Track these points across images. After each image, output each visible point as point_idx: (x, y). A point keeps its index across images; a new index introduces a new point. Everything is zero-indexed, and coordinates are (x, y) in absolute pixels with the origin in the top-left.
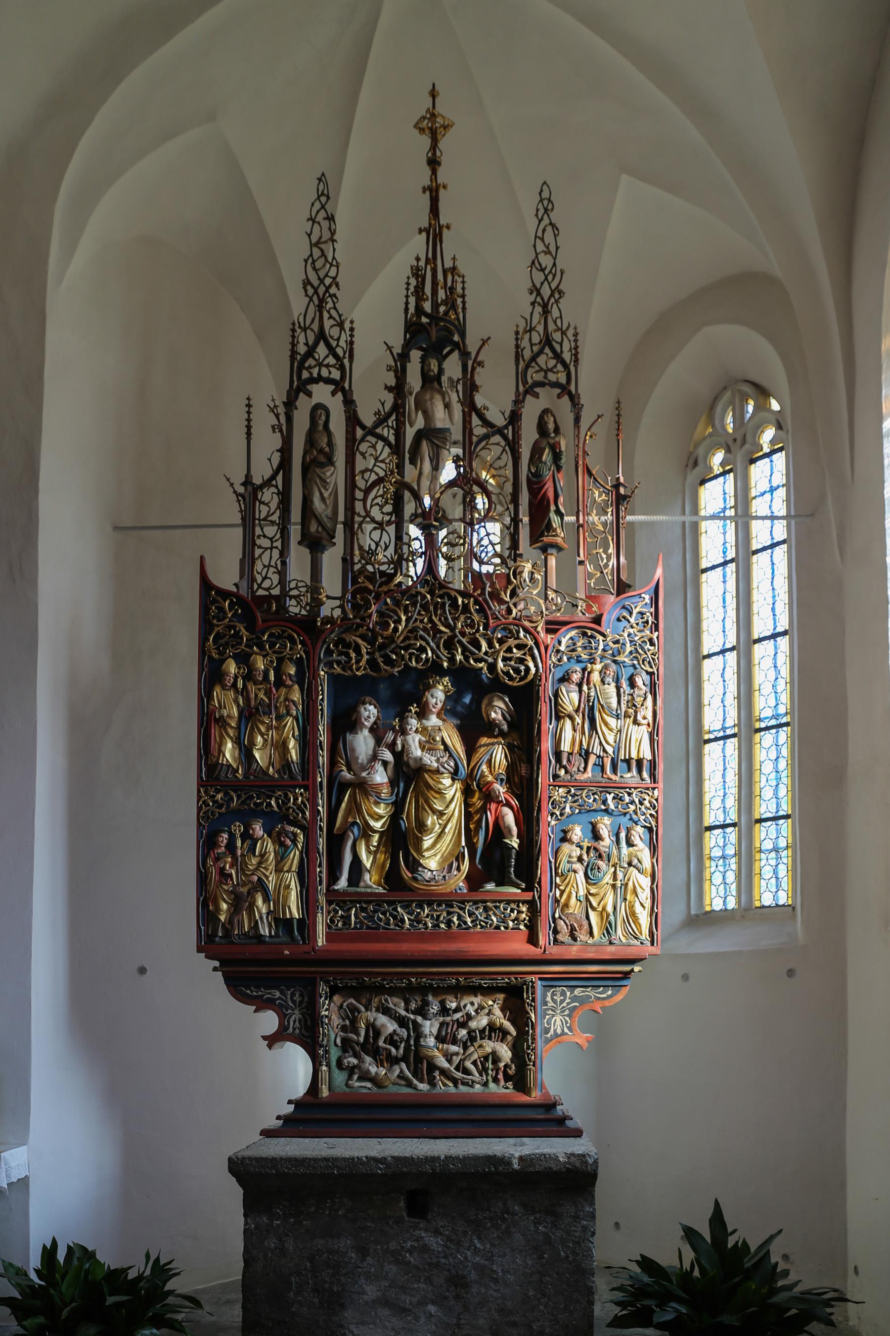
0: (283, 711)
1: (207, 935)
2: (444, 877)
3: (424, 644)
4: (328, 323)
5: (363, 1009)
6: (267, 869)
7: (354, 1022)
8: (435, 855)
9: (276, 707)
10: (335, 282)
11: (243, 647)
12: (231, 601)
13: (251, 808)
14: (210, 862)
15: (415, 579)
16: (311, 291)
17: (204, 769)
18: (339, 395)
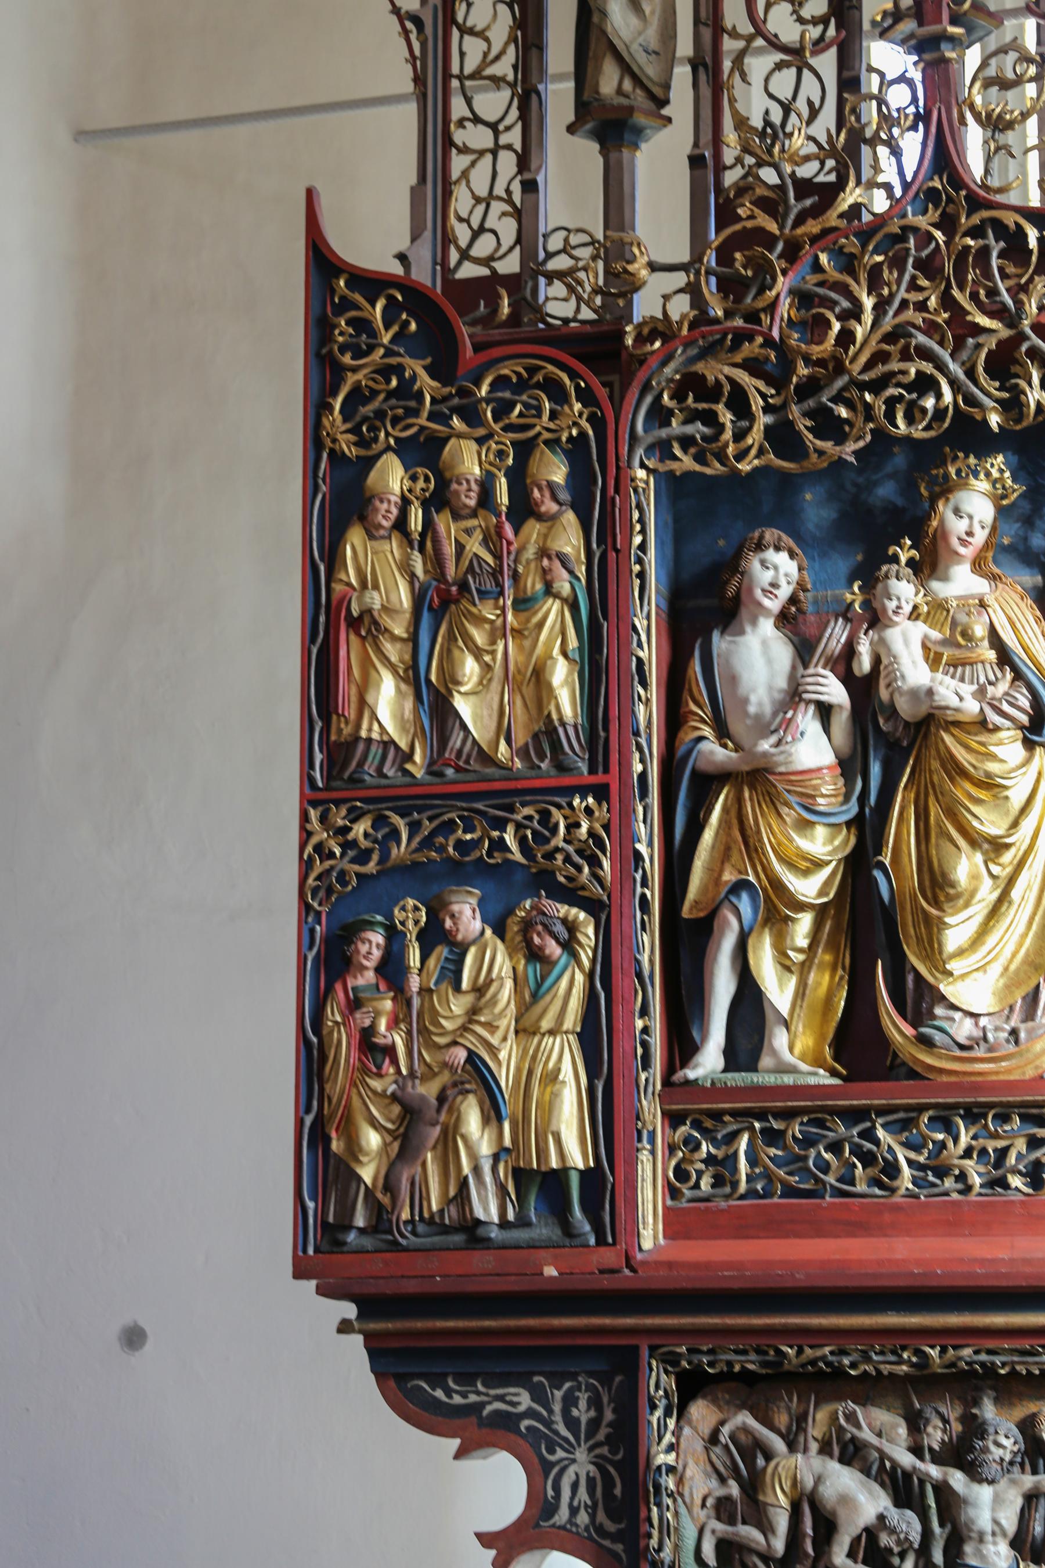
0: (533, 584)
1: (325, 1226)
2: (1014, 1032)
3: (928, 368)
5: (779, 1444)
6: (491, 1027)
7: (753, 1485)
9: (515, 576)
11: (423, 421)
12: (391, 299)
13: (450, 859)
14: (333, 1014)
15: (898, 192)
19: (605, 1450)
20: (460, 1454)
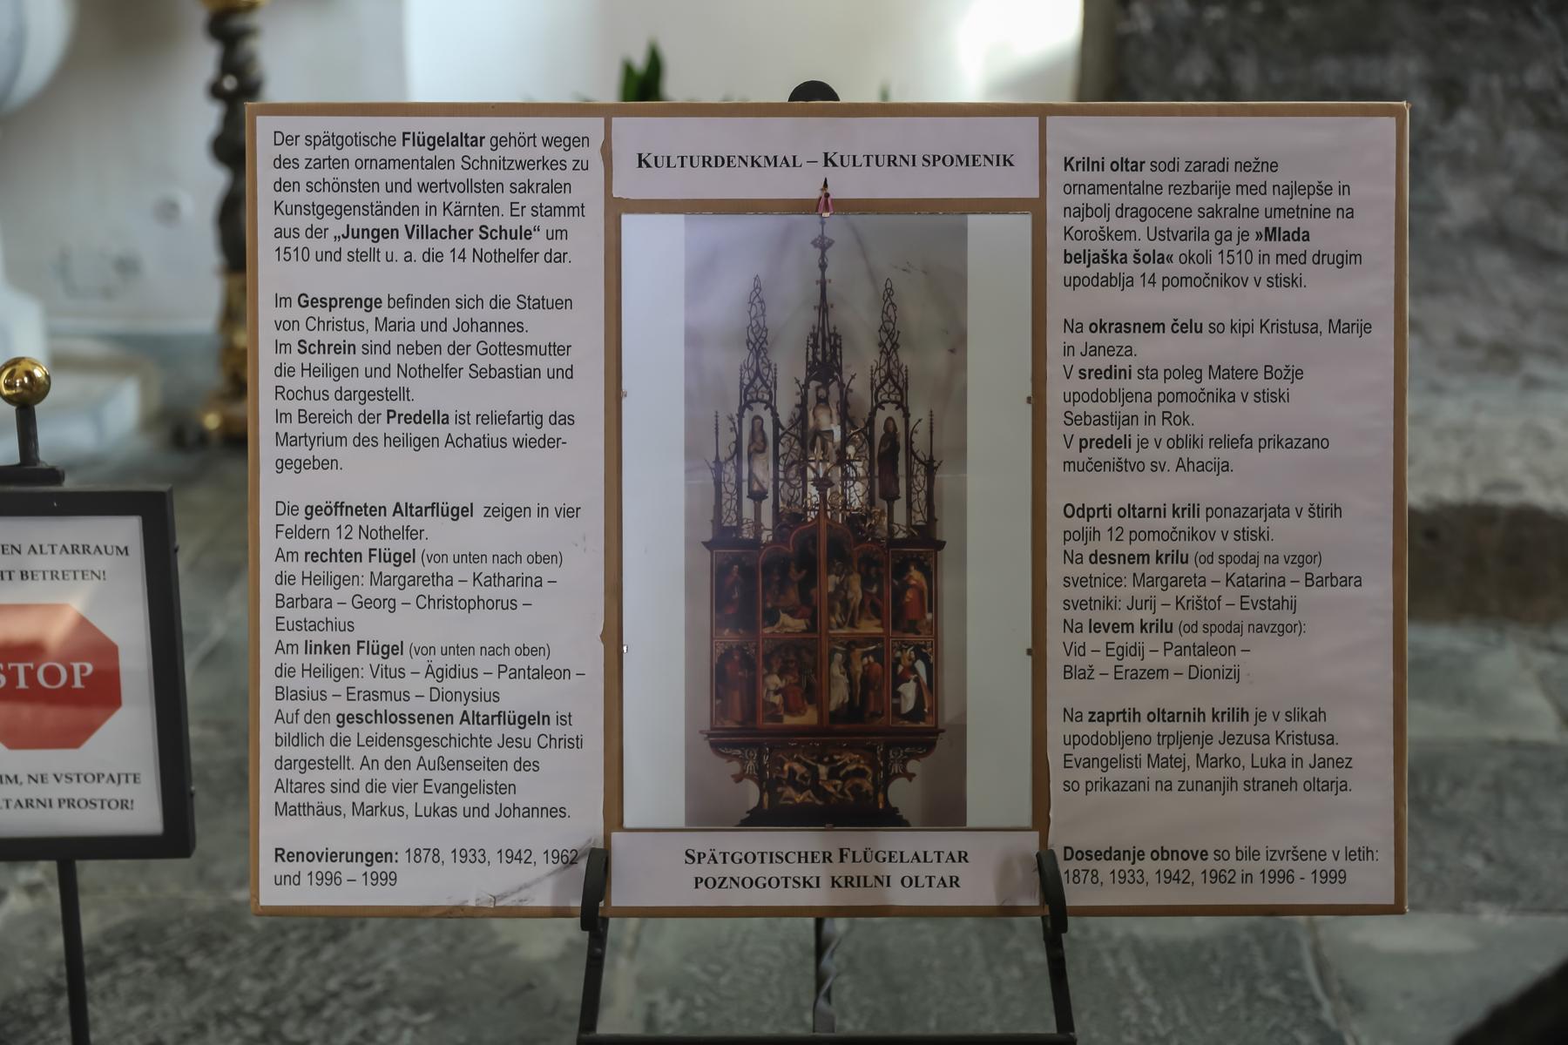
10: (765, 340)
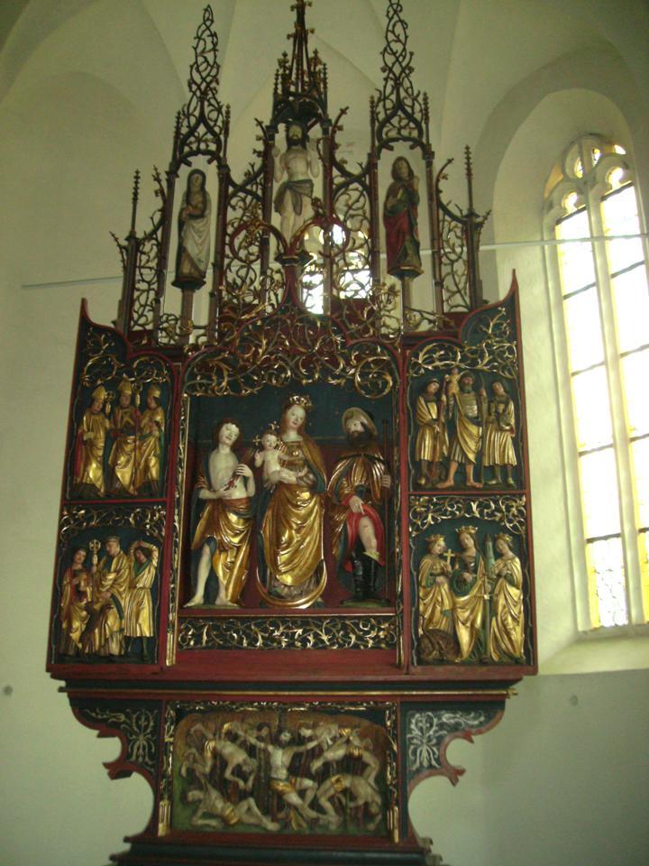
4: (207, 109)
5: (210, 736)
8: (292, 570)
16: (194, 87)
17: (68, 489)
18: (215, 163)
19: (149, 736)
20: (99, 736)
